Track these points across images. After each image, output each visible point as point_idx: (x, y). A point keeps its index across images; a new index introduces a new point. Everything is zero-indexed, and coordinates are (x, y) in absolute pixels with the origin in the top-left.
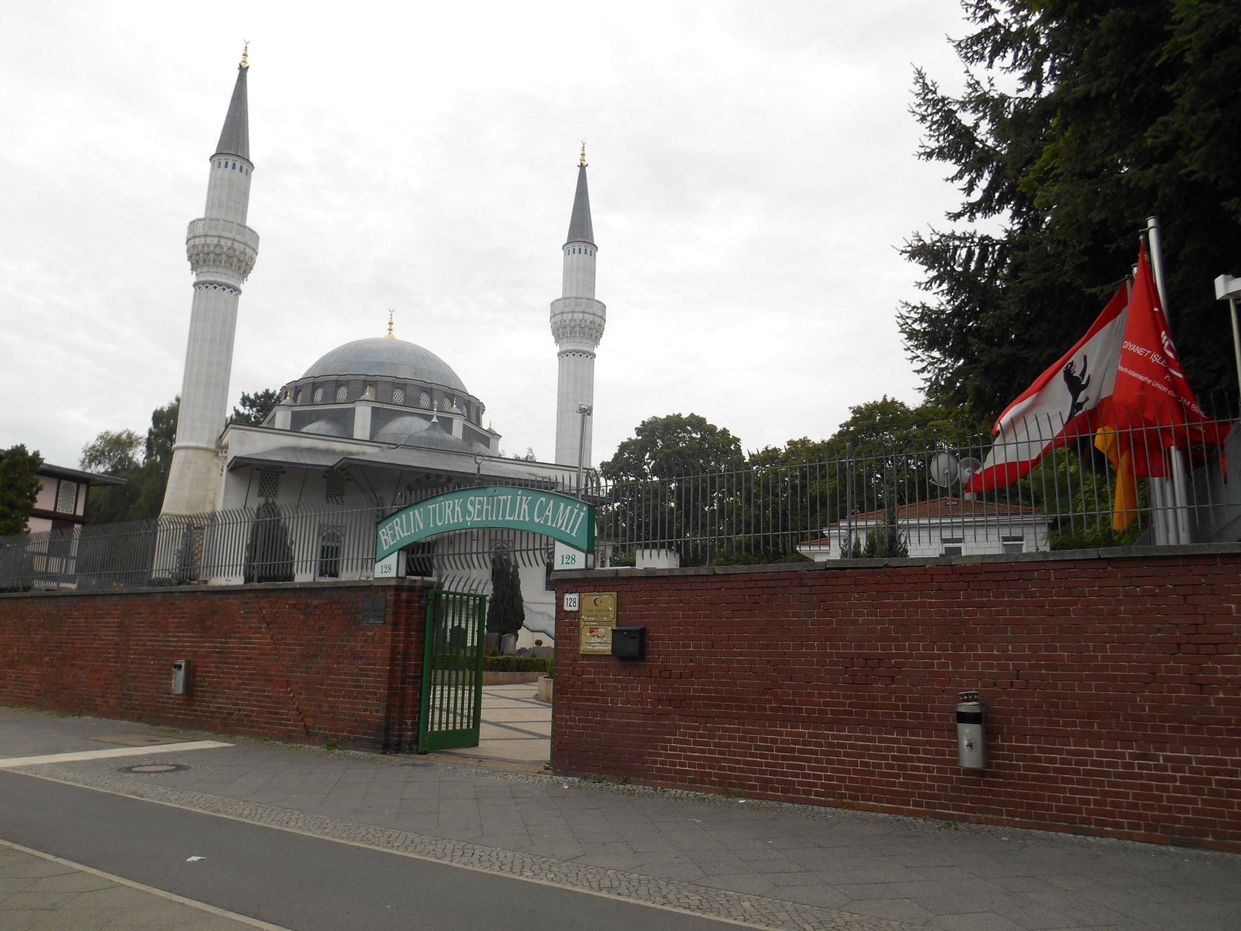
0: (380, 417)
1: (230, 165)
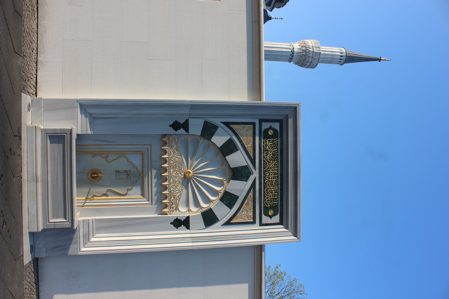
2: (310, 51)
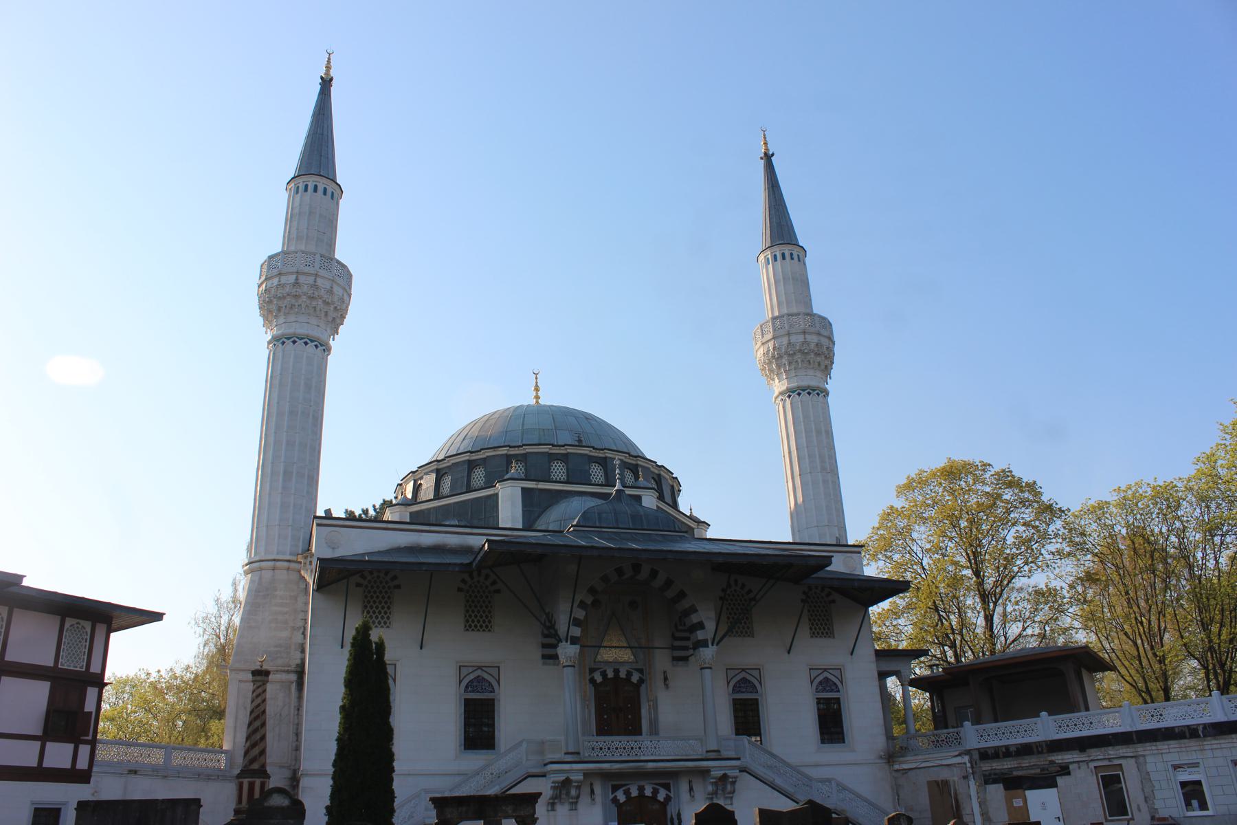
0: (534, 504)
1: (311, 188)
2: (774, 349)
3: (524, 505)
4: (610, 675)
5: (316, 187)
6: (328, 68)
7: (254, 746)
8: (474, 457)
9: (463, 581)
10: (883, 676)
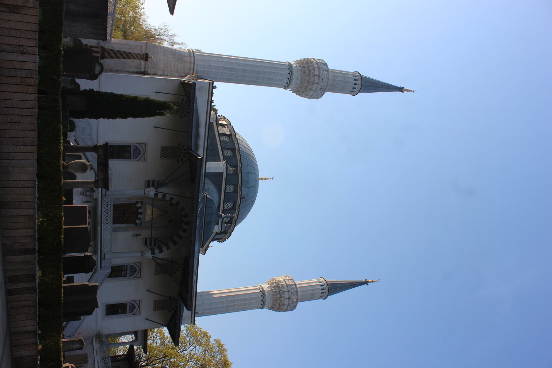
0: (216, 177)
3: (215, 173)
4: (140, 211)
5: (356, 84)
6: (408, 91)
7: (115, 53)
8: (237, 151)
9: (183, 146)
10: (135, 333)
